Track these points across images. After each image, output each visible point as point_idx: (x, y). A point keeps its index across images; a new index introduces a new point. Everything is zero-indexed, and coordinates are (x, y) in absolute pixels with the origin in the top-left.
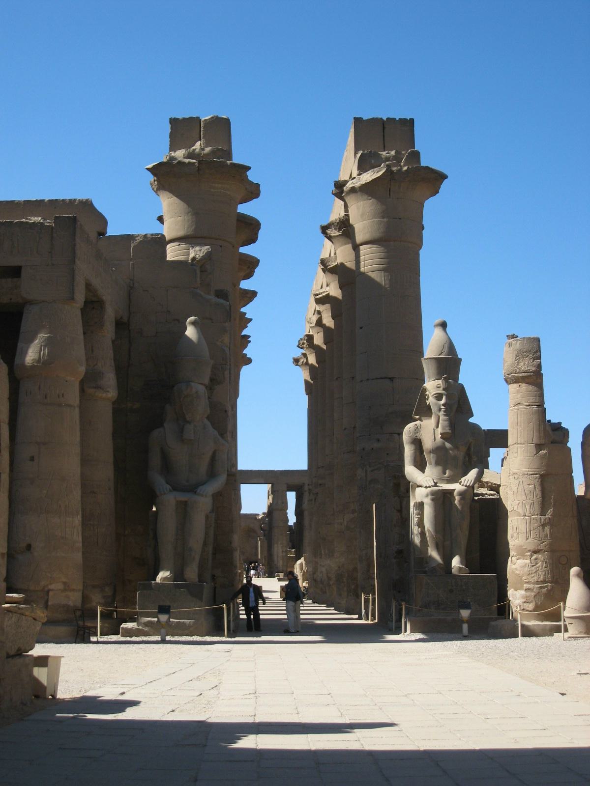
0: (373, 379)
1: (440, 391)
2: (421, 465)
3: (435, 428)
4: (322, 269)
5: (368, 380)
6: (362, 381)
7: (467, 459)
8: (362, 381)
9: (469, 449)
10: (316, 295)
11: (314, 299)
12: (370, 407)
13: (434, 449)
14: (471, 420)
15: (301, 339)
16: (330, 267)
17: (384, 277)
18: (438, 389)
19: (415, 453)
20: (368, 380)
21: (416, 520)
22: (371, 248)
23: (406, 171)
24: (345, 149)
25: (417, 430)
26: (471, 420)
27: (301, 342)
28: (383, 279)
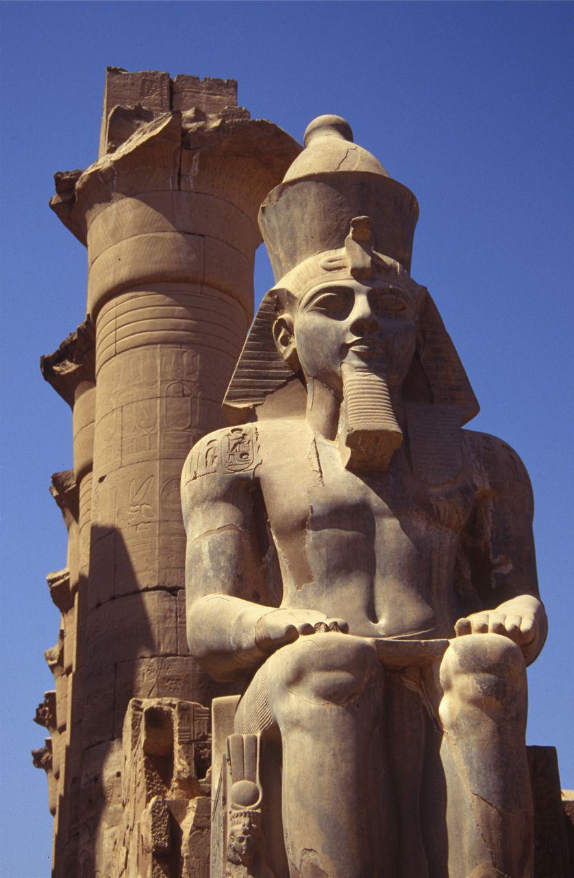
0: (126, 595)
1: (344, 279)
2: (255, 577)
3: (321, 439)
4: (56, 498)
5: (113, 598)
6: (99, 605)
7: (467, 574)
8: (99, 605)
9: (472, 528)
10: (52, 581)
11: (49, 589)
12: (116, 665)
13: (316, 509)
14: (469, 426)
15: (41, 706)
16: (69, 489)
17: (162, 356)
18: (329, 274)
19: (240, 548)
20: (113, 598)
21: (238, 826)
22: (132, 297)
23: (217, 129)
24: (91, 164)
25: (240, 449)
26: (469, 426)
27: (41, 711)
28: (159, 361)
